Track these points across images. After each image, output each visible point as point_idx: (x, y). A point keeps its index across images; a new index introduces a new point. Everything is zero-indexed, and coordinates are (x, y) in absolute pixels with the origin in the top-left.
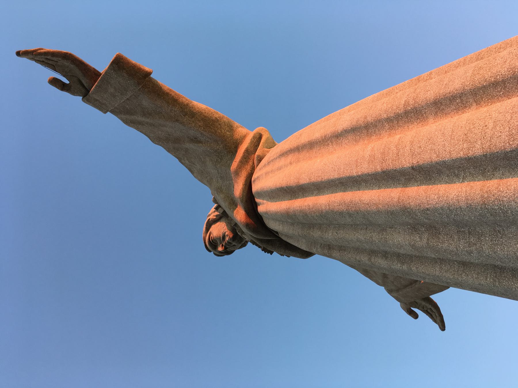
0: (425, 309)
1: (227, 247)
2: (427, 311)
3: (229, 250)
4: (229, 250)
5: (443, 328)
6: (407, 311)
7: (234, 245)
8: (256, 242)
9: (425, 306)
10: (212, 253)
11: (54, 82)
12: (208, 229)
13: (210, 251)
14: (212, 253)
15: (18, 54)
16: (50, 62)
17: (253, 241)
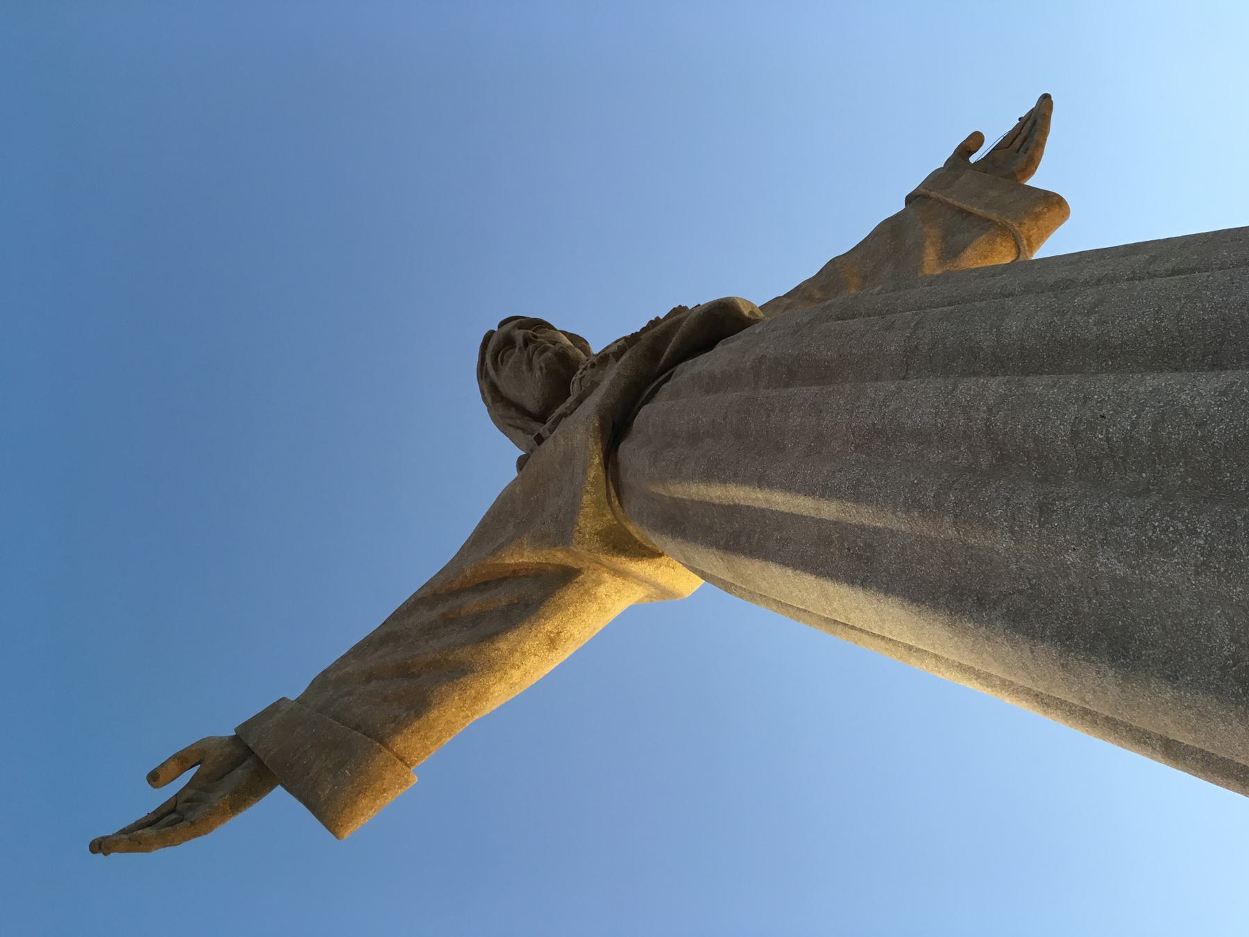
0: (179, 808)
1: (531, 347)
2: (173, 811)
3: (508, 353)
4: (512, 354)
5: (99, 846)
8: (658, 327)
9: (195, 804)
10: (496, 329)
11: (976, 139)
12: (562, 332)
13: (502, 324)
14: (496, 329)
15: (1046, 99)
16: (1018, 142)
17: (659, 324)
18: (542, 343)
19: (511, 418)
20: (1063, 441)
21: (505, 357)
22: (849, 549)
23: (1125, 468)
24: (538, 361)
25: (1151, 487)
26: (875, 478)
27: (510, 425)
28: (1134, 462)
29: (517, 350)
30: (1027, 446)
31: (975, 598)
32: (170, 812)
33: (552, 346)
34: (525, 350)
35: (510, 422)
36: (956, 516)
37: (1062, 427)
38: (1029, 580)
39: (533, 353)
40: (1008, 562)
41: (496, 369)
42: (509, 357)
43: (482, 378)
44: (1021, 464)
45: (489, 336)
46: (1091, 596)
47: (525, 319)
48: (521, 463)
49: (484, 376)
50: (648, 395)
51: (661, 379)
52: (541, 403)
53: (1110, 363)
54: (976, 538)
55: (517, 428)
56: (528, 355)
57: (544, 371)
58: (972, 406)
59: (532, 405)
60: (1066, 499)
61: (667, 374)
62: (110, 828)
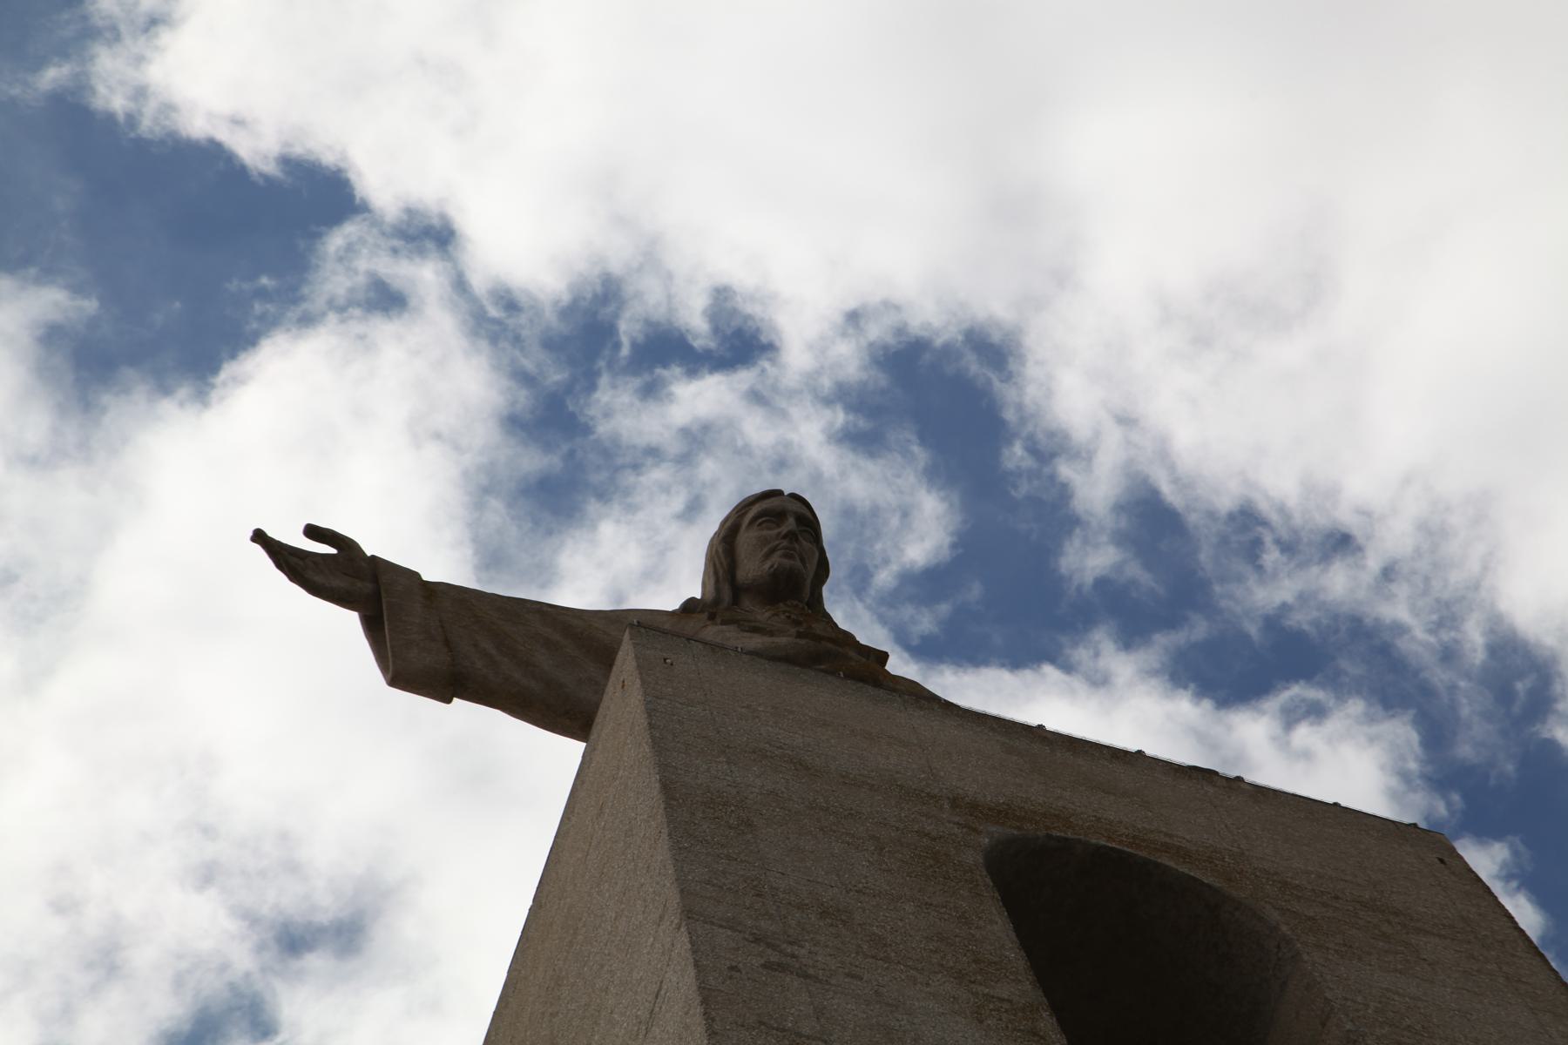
2: (302, 559)
5: (259, 537)
7: (773, 551)
13: (794, 496)
18: (794, 549)
19: (721, 563)
21: (764, 525)
24: (776, 559)
29: (776, 531)
35: (717, 563)
39: (781, 549)
42: (769, 529)
43: (737, 512)
48: (690, 606)
52: (746, 582)
55: (716, 573)
56: (778, 545)
62: (271, 533)
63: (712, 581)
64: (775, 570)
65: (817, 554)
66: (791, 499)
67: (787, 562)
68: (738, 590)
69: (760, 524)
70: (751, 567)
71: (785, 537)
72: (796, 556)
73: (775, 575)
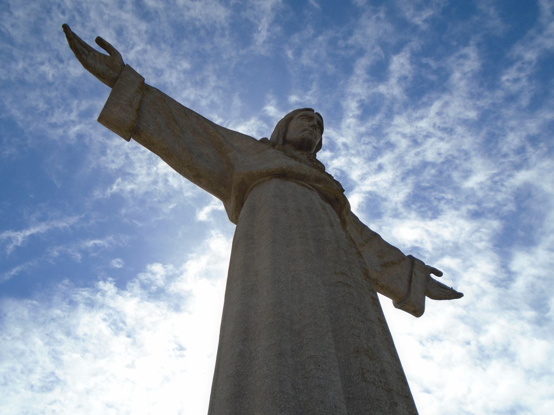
1: (311, 129)
2: (89, 51)
3: (306, 120)
6: (113, 51)
7: (305, 130)
10: (315, 112)
11: (439, 274)
13: (317, 114)
14: (315, 112)
16: (442, 290)
20: (308, 353)
21: (304, 119)
22: (255, 284)
23: (303, 378)
24: (306, 134)
25: (297, 390)
26: (282, 288)
27: (279, 130)
28: (305, 381)
29: (308, 123)
30: (305, 341)
31: (246, 337)
32: (88, 50)
33: (314, 137)
34: (310, 127)
36: (273, 323)
37: (313, 352)
38: (256, 356)
39: (309, 130)
40: (260, 346)
41: (299, 117)
44: (298, 340)
45: (311, 110)
46: (254, 380)
47: (321, 122)
48: (264, 140)
49: (295, 113)
50: (302, 184)
51: (309, 186)
53: (343, 360)
54: (266, 332)
55: (279, 133)
57: (303, 137)
58: (316, 316)
59: (289, 136)
60: (286, 362)
61: (312, 188)
63: (276, 135)
64: (305, 137)
65: (320, 139)
66: (316, 114)
67: (310, 137)
68: (285, 142)
69: (303, 119)
70: (294, 134)
71: (311, 126)
72: (314, 135)
73: (303, 140)
